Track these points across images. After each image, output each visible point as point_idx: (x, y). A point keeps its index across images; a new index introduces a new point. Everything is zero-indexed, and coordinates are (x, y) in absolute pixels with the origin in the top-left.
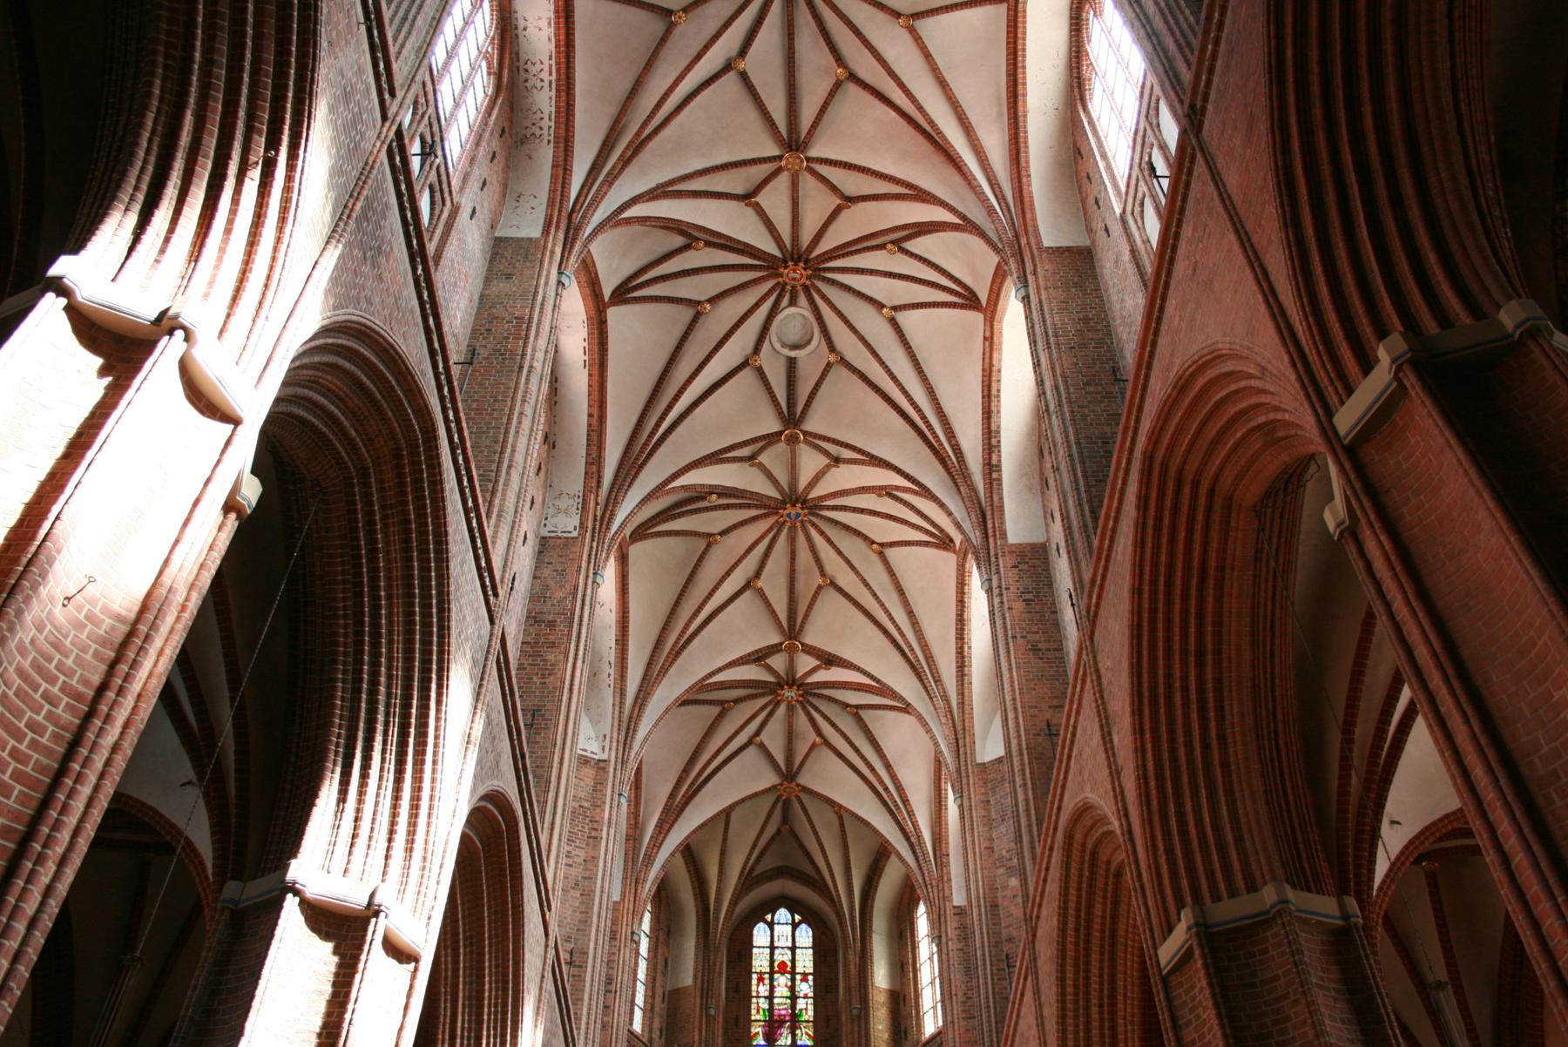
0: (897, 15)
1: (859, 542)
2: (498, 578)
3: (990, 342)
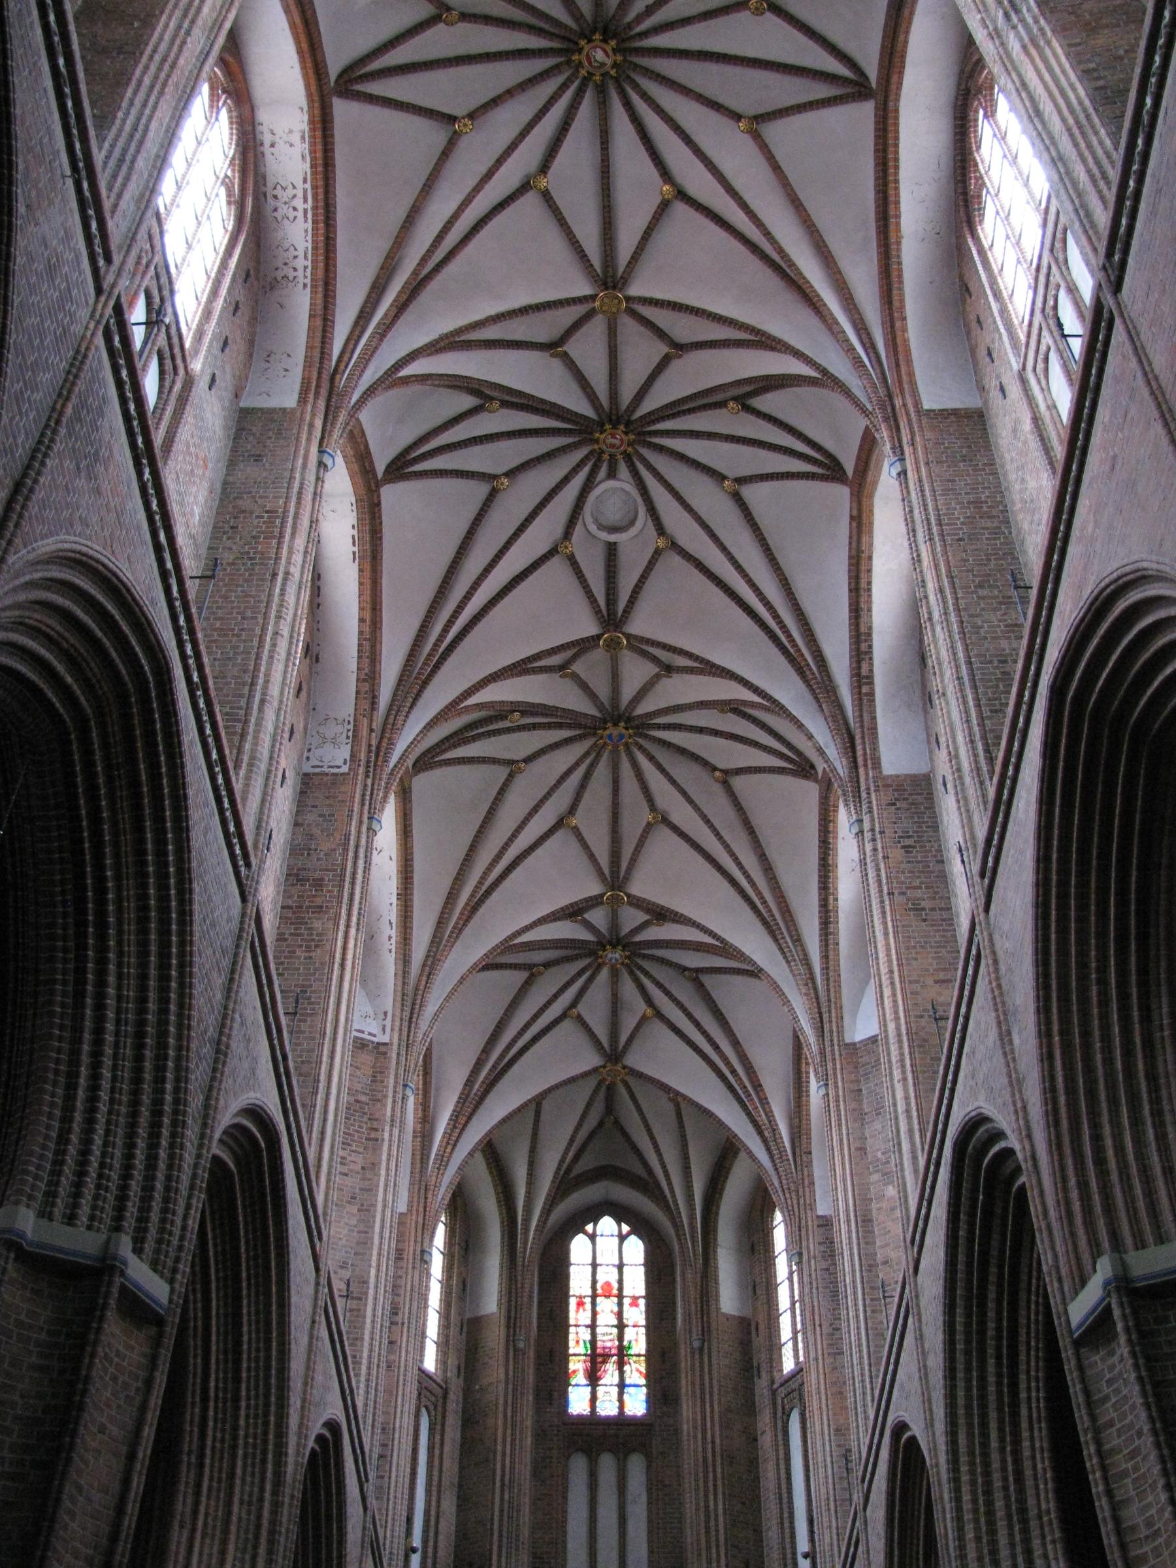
0: (737, 117)
1: (696, 768)
2: (250, 844)
3: (860, 523)
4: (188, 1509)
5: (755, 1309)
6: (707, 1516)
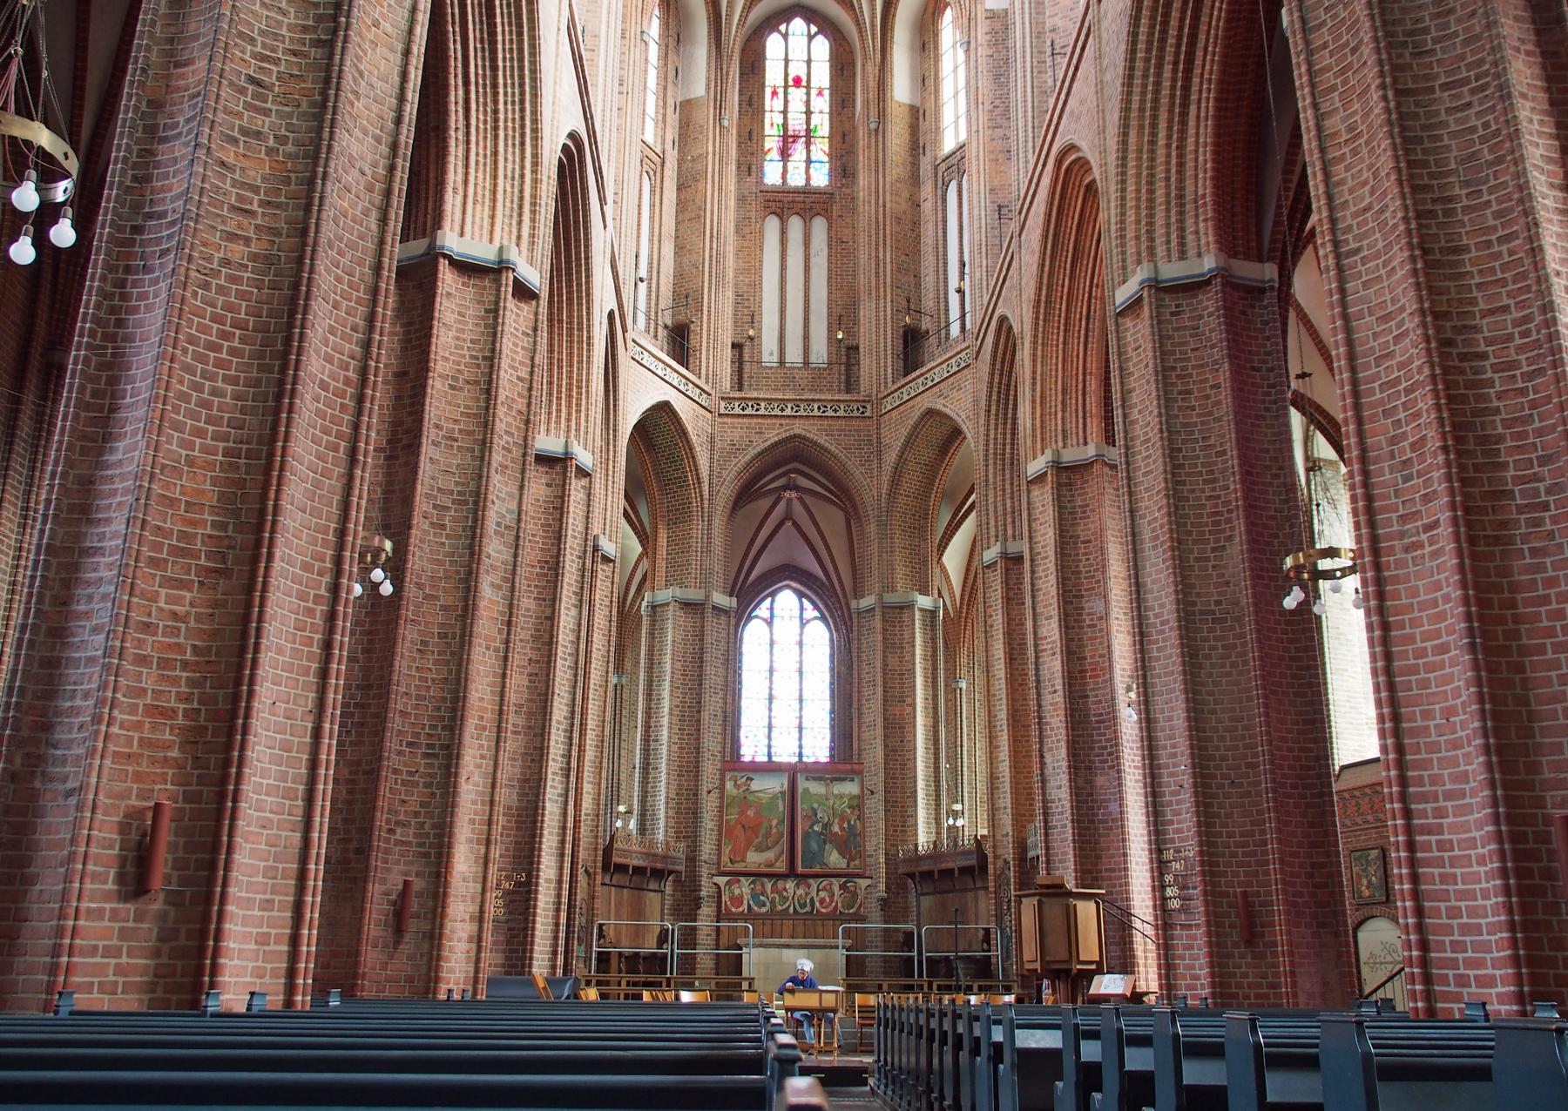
4: (460, 178)
5: (923, 98)
6: (877, 265)
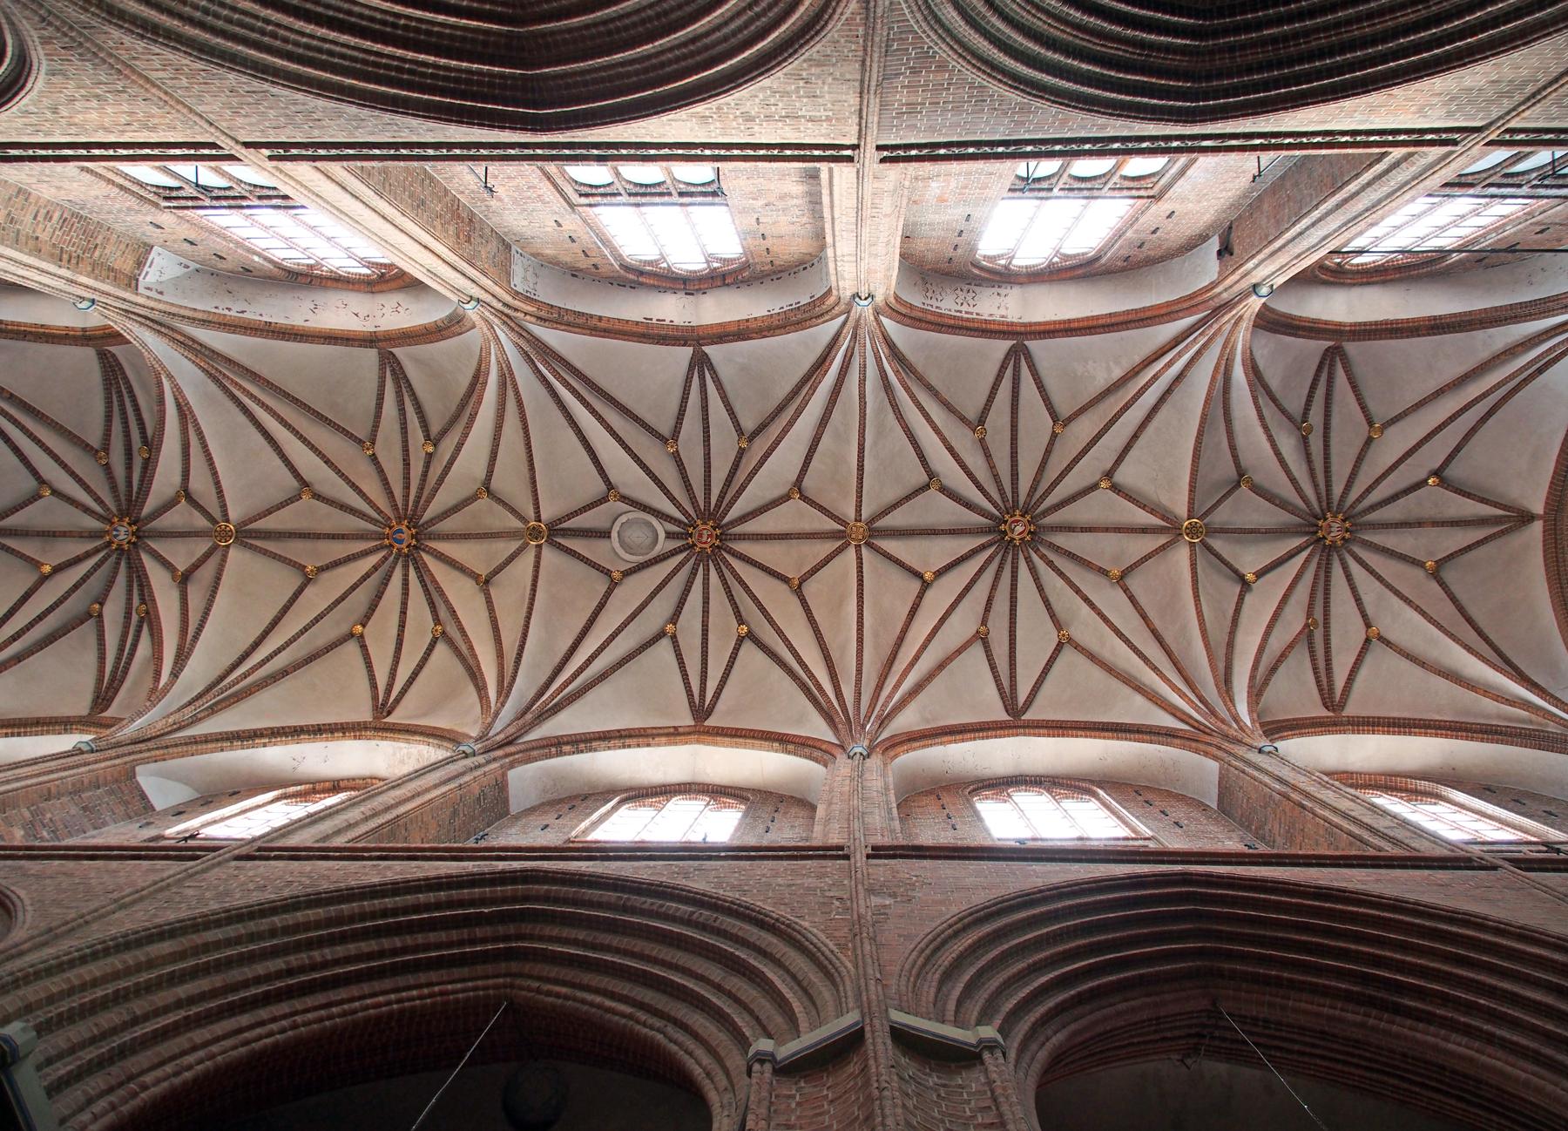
0: (984, 622)
